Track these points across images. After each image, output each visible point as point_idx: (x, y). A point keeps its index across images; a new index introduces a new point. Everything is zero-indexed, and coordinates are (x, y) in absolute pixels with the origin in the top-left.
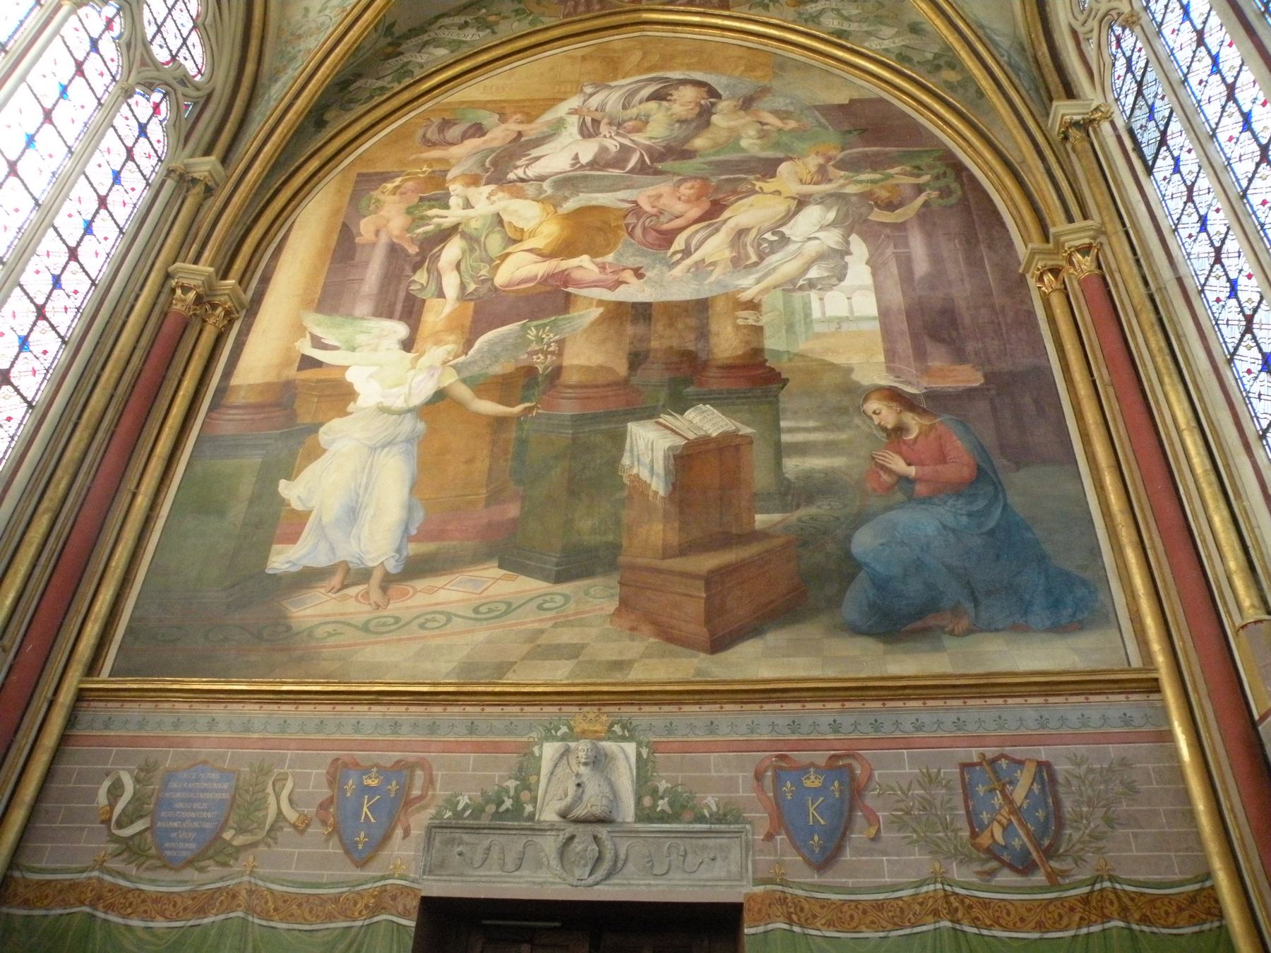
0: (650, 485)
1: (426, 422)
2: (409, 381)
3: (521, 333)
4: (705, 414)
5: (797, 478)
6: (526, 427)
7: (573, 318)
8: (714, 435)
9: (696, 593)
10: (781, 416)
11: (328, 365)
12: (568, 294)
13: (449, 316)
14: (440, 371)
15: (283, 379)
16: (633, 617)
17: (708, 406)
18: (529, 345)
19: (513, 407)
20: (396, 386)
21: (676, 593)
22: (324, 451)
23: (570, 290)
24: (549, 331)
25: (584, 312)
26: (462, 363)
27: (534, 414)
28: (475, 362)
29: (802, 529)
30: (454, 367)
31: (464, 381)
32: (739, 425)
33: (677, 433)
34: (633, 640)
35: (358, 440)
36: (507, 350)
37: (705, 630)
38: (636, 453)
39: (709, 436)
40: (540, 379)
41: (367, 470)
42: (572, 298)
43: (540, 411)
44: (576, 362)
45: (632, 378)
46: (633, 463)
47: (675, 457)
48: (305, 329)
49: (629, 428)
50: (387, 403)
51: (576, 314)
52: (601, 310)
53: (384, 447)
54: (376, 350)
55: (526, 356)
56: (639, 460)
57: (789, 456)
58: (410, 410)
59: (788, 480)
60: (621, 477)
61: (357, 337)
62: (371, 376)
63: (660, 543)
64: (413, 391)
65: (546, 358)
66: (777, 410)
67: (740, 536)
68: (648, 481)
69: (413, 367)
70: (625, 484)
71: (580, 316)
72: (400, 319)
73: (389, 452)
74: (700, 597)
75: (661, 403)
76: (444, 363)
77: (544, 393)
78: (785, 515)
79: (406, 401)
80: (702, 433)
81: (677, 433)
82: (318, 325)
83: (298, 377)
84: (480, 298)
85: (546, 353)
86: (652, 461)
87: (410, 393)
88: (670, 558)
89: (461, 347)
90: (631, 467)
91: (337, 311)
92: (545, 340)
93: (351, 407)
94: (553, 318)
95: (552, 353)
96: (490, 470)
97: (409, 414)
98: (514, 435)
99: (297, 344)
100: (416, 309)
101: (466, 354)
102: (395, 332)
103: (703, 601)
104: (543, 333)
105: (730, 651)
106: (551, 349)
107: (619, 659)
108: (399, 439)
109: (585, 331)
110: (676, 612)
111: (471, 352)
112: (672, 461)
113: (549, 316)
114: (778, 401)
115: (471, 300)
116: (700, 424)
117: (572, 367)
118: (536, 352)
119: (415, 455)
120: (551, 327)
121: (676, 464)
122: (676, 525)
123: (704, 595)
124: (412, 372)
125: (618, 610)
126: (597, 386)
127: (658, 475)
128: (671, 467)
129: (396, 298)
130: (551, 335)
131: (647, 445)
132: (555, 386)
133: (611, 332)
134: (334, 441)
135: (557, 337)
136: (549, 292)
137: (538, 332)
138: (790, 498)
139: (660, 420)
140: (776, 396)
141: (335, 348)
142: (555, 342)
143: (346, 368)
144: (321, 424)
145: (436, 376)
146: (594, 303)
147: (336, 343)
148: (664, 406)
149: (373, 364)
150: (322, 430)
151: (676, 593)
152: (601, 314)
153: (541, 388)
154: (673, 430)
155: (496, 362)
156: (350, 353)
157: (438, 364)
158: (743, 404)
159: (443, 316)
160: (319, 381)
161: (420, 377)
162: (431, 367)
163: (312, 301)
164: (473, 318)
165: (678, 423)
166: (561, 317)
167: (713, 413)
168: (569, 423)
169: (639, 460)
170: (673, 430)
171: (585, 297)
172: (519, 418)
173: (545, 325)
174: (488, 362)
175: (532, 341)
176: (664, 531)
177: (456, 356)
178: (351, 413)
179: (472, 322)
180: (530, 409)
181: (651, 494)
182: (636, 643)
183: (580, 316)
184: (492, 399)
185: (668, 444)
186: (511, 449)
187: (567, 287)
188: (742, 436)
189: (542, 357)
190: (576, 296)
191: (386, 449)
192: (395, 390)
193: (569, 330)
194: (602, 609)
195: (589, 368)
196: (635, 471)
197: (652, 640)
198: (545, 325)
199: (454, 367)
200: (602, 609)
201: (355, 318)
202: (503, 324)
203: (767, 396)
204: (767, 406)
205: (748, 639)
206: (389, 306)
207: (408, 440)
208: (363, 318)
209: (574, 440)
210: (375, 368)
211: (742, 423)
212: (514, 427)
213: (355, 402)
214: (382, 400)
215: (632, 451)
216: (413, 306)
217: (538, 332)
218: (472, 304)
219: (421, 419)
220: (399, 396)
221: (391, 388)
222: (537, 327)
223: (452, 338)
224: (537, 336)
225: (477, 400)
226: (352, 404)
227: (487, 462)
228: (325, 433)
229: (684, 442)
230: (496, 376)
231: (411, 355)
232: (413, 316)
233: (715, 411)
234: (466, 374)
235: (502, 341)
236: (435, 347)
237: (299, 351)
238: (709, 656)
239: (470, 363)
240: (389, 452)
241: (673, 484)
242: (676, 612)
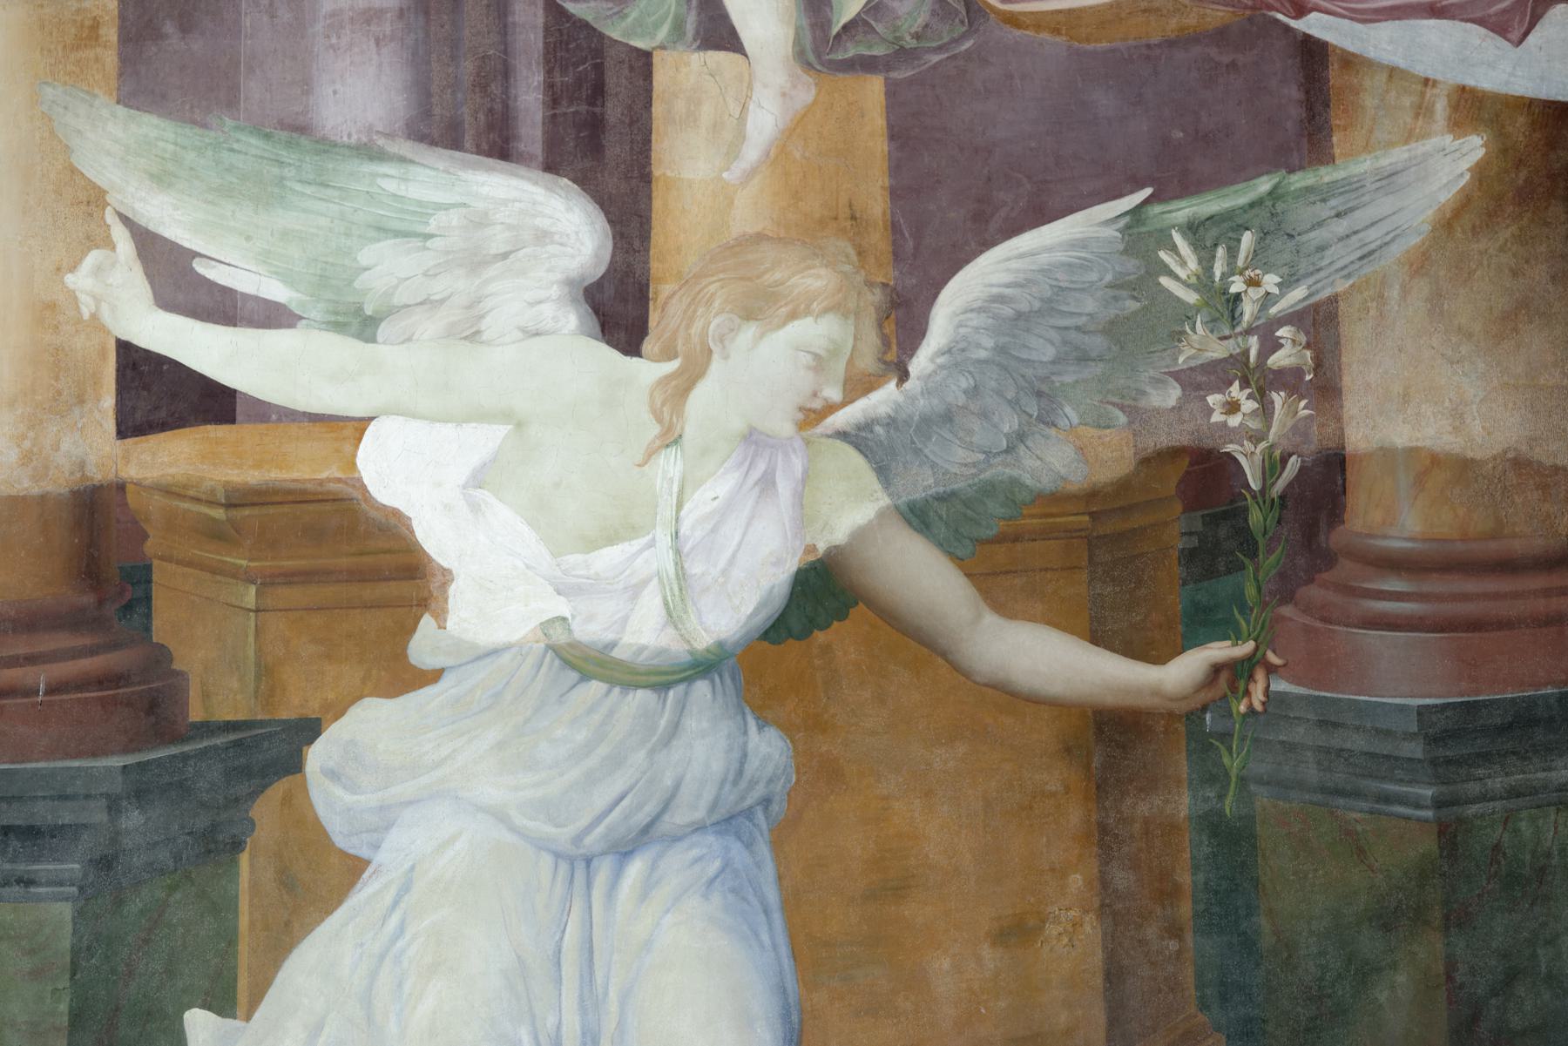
1: (787, 729)
2: (666, 511)
3: (1132, 265)
6: (1233, 764)
7: (1351, 187)
11: (263, 412)
12: (1313, 53)
13: (779, 154)
14: (798, 464)
15: (58, 483)
18: (1179, 336)
19: (1160, 659)
20: (611, 539)
22: (355, 868)
23: (1314, 25)
24: (1259, 257)
25: (1399, 155)
26: (891, 422)
27: (1258, 697)
28: (948, 417)
30: (856, 437)
31: (918, 516)
35: (500, 816)
36: (1084, 358)
40: (1255, 517)
41: (570, 970)
42: (1334, 74)
43: (1280, 686)
44: (1401, 435)
48: (95, 198)
50: (590, 630)
51: (1362, 166)
52: (1474, 148)
53: (623, 850)
54: (474, 337)
55: (1172, 395)
58: (703, 667)
61: (365, 256)
62: (478, 479)
64: (695, 568)
65: (1266, 410)
69: (671, 438)
71: (1388, 179)
72: (551, 167)
73: (646, 891)
76: (811, 416)
77: (1287, 597)
79: (672, 617)
82: (161, 179)
83: (132, 472)
84: (903, 55)
85: (1263, 382)
87: (682, 575)
89: (871, 338)
91: (231, 103)
92: (1248, 309)
93: (424, 646)
94: (1264, 185)
95: (1288, 380)
96: (1114, 975)
97: (702, 688)
98: (1184, 805)
99: (80, 281)
100: (613, 111)
101: (904, 376)
102: (542, 237)
104: (1232, 270)
106: (1279, 359)
108: (680, 817)
109: (1420, 263)
111: (921, 363)
113: (1241, 172)
115: (867, 65)
117: (1387, 454)
118: (1217, 375)
119: (772, 895)
120: (1264, 235)
124: (670, 465)
126: (1506, 566)
129: (506, 49)
130: (1271, 281)
132: (1328, 559)
133: (1539, 273)
134: (385, 819)
135: (1297, 294)
136: (1220, 36)
137: (1207, 263)
141: (272, 316)
142: (1295, 318)
143: (359, 425)
144: (310, 729)
145: (785, 488)
146: (1441, 107)
147: (276, 291)
149: (481, 416)
150: (317, 756)
152: (1480, 171)
153: (1270, 562)
155: (1046, 420)
156: (341, 349)
157: (783, 425)
159: (752, 153)
160: (239, 499)
161: (702, 501)
162: (753, 440)
163: (90, 33)
164: (895, 169)
166: (1299, 180)
168: (1415, 749)
171: (1393, 72)
172: (1193, 717)
173: (1227, 227)
174: (1009, 423)
175: (1186, 315)
177: (858, 386)
178: (434, 676)
179: (895, 194)
180: (1234, 674)
183: (1388, 179)
184: (1059, 620)
186: (1185, 878)
187: (1301, 11)
189: (1249, 406)
190: (1350, 61)
191: (636, 868)
192: (608, 558)
193: (1341, 255)
195: (1463, 468)
198: (1227, 227)
199: (856, 437)
201: (327, 146)
202: (1040, 215)
206: (481, 85)
207: (728, 822)
208: (368, 151)
209: (1450, 835)
210: (498, 432)
212: (1182, 765)
213: (441, 618)
214: (562, 607)
216: (598, 91)
217: (1207, 263)
218: (874, 88)
219: (763, 723)
220: (635, 591)
221: (591, 544)
222: (1193, 229)
223: (817, 280)
224: (1203, 283)
225: (990, 619)
226: (427, 622)
227: (1091, 928)
228: (333, 775)
230: (1056, 499)
231: (646, 371)
232: (615, 148)
234: (921, 483)
235: (1049, 307)
236: (749, 331)
237: (96, 323)
239: (927, 424)
240: (646, 891)
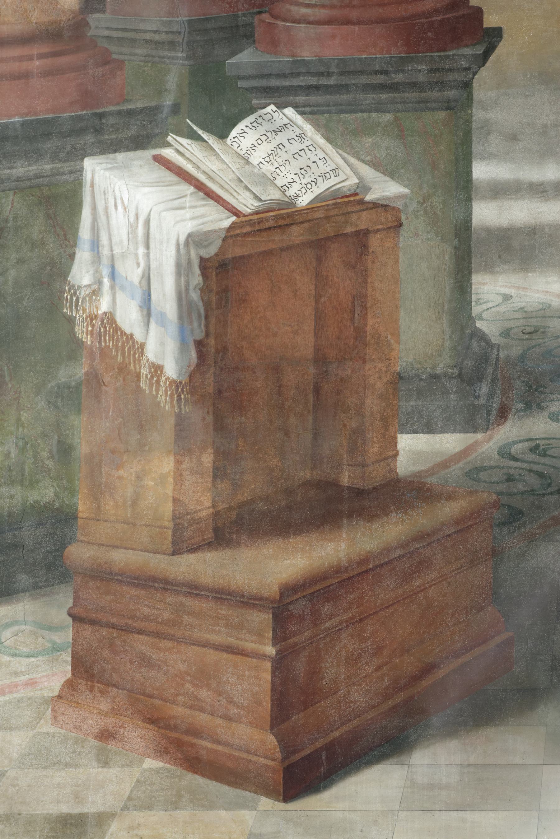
0: (142, 346)
4: (281, 138)
5: (506, 333)
8: (304, 201)
9: (249, 646)
10: (477, 148)
16: (105, 705)
17: (290, 111)
21: (206, 645)
29: (510, 479)
32: (368, 172)
33: (210, 194)
34: (106, 764)
37: (271, 740)
38: (105, 252)
39: (291, 204)
45: (94, 19)
46: (100, 282)
47: (204, 263)
49: (88, 176)
56: (113, 276)
57: (489, 268)
59: (481, 336)
60: (71, 321)
63: (168, 509)
66: (468, 134)
67: (359, 493)
68: (139, 336)
70: (80, 343)
74: (263, 657)
75: (168, 101)
78: (470, 438)
80: (274, 195)
81: (210, 194)
86: (147, 278)
88: (192, 550)
90: (96, 293)
103: (268, 665)
105: (326, 795)
107: (76, 810)
110: (204, 694)
112: (197, 279)
114: (470, 98)
116: (268, 169)
121: (204, 290)
122: (208, 459)
123: (270, 650)
125: (70, 685)
127: (162, 321)
128: (195, 296)
131: (133, 228)
138: (484, 389)
139: (168, 153)
140: (467, 85)
148: (176, 109)
151: (206, 645)
154: (200, 186)
158: (379, 108)
165: (212, 165)
167: (301, 137)
169: (113, 276)
170: (200, 186)
176: (179, 477)
181: (144, 371)
182: (113, 772)
185: (189, 227)
188: (375, 205)
194: (32, 683)
196: (104, 306)
197: (150, 763)
200: (32, 683)
203: (441, 85)
204: (442, 115)
205: (370, 763)
211: (375, 165)
215: (95, 245)
229: (229, 221)
233: (308, 128)
238: (281, 806)
241: (200, 344)
242: (204, 694)
